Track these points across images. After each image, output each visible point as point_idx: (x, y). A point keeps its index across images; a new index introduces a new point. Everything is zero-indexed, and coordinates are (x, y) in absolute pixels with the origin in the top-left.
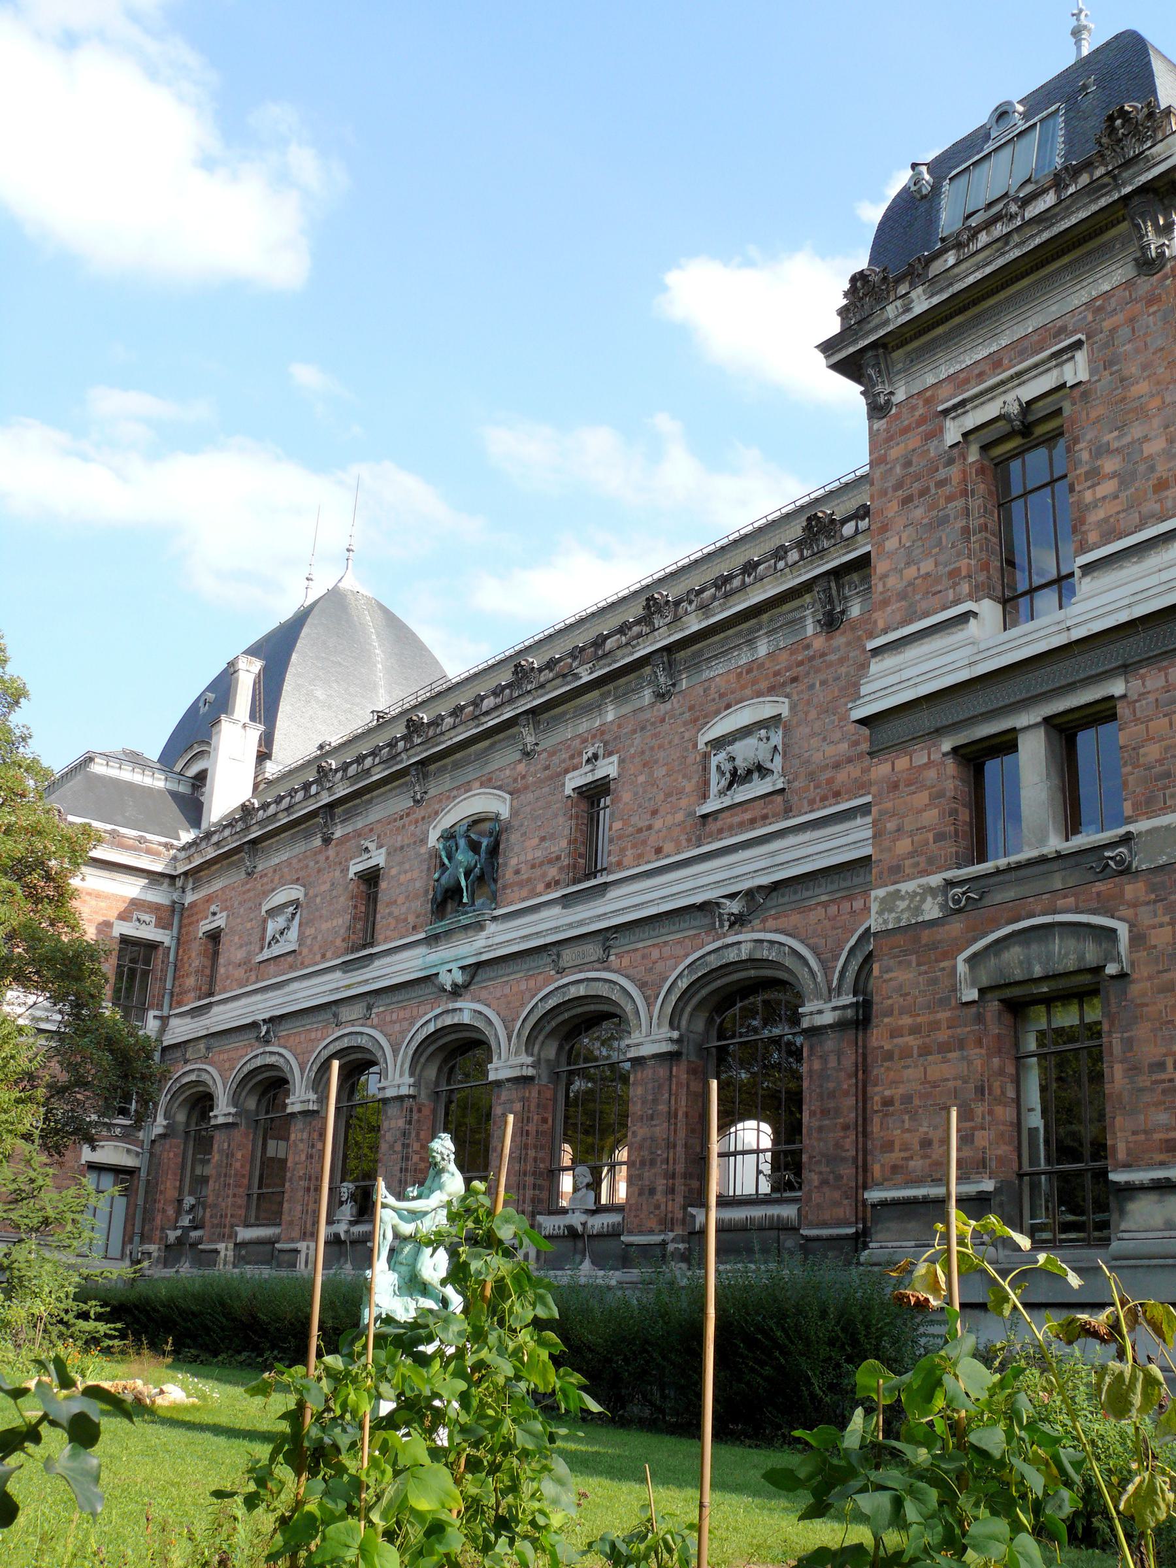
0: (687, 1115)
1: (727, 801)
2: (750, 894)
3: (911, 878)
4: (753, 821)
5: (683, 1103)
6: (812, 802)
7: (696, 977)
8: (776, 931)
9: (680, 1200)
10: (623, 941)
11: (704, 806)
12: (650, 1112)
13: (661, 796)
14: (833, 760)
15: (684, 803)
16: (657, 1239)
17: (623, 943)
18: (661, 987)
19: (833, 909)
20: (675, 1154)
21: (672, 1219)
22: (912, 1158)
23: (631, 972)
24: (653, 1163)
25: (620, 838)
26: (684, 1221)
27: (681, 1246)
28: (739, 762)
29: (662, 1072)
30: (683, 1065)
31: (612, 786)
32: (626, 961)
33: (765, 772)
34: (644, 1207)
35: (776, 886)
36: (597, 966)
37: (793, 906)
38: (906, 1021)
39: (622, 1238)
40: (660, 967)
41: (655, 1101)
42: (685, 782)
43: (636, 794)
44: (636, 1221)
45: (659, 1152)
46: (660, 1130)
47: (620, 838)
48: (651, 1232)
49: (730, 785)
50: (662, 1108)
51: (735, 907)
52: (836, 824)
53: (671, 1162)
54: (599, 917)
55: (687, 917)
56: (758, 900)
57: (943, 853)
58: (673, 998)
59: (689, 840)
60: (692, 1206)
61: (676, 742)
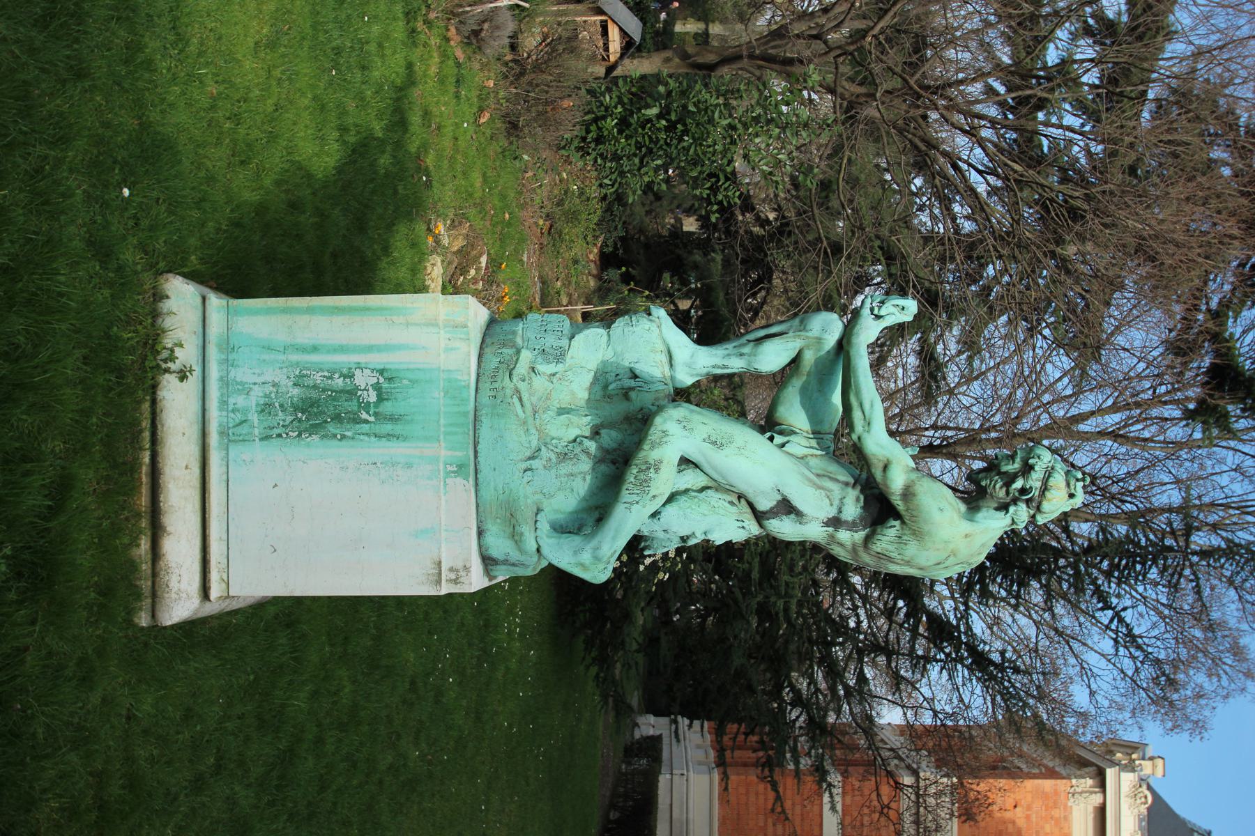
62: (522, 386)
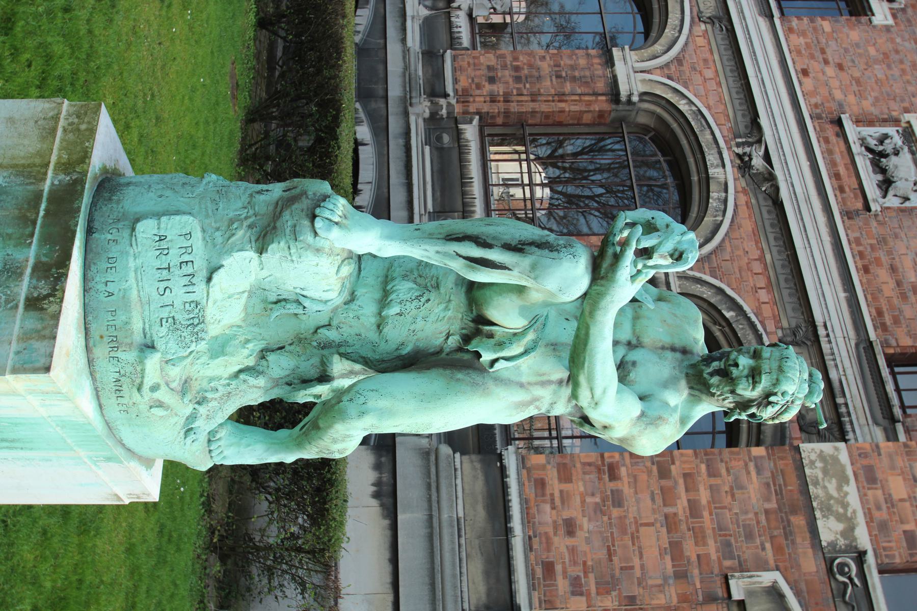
0: (562, 111)
1: (856, 148)
2: (771, 177)
3: (863, 497)
4: (837, 176)
5: (573, 108)
6: (858, 241)
7: (690, 120)
8: (736, 205)
9: (485, 108)
10: (719, 37)
11: (850, 123)
12: (564, 74)
13: (857, 74)
14: (899, 265)
15: (851, 99)
16: (450, 90)
17: (717, 38)
18: (678, 82)
19: (757, 267)
20: (526, 101)
21: (468, 102)
22: (553, 508)
23: (691, 47)
24: (518, 79)
25: (815, 29)
26: (466, 113)
27: (444, 112)
28: (894, 160)
29: (600, 86)
30: (606, 107)
31: (864, 19)
32: (701, 41)
33: (884, 187)
34: (478, 73)
35: (778, 205)
36: (695, 10)
37: (760, 223)
38: (704, 496)
39: (449, 51)
40: (697, 78)
41: (574, 79)
42: (871, 100)
43: (857, 45)
44: (465, 64)
45: (528, 86)
46: (548, 86)
47: (815, 29)
48: (455, 81)
49: (869, 149)
50: (568, 87)
51: (758, 162)
52: (838, 268)
53: (520, 98)
54: (741, 12)
55: (745, 107)
56: (764, 185)
57: (893, 544)
58: (669, 96)
59: (816, 106)
60: (480, 119)
61: (910, 88)
62: (160, 395)
